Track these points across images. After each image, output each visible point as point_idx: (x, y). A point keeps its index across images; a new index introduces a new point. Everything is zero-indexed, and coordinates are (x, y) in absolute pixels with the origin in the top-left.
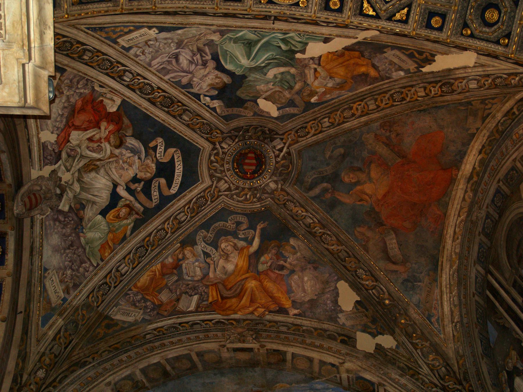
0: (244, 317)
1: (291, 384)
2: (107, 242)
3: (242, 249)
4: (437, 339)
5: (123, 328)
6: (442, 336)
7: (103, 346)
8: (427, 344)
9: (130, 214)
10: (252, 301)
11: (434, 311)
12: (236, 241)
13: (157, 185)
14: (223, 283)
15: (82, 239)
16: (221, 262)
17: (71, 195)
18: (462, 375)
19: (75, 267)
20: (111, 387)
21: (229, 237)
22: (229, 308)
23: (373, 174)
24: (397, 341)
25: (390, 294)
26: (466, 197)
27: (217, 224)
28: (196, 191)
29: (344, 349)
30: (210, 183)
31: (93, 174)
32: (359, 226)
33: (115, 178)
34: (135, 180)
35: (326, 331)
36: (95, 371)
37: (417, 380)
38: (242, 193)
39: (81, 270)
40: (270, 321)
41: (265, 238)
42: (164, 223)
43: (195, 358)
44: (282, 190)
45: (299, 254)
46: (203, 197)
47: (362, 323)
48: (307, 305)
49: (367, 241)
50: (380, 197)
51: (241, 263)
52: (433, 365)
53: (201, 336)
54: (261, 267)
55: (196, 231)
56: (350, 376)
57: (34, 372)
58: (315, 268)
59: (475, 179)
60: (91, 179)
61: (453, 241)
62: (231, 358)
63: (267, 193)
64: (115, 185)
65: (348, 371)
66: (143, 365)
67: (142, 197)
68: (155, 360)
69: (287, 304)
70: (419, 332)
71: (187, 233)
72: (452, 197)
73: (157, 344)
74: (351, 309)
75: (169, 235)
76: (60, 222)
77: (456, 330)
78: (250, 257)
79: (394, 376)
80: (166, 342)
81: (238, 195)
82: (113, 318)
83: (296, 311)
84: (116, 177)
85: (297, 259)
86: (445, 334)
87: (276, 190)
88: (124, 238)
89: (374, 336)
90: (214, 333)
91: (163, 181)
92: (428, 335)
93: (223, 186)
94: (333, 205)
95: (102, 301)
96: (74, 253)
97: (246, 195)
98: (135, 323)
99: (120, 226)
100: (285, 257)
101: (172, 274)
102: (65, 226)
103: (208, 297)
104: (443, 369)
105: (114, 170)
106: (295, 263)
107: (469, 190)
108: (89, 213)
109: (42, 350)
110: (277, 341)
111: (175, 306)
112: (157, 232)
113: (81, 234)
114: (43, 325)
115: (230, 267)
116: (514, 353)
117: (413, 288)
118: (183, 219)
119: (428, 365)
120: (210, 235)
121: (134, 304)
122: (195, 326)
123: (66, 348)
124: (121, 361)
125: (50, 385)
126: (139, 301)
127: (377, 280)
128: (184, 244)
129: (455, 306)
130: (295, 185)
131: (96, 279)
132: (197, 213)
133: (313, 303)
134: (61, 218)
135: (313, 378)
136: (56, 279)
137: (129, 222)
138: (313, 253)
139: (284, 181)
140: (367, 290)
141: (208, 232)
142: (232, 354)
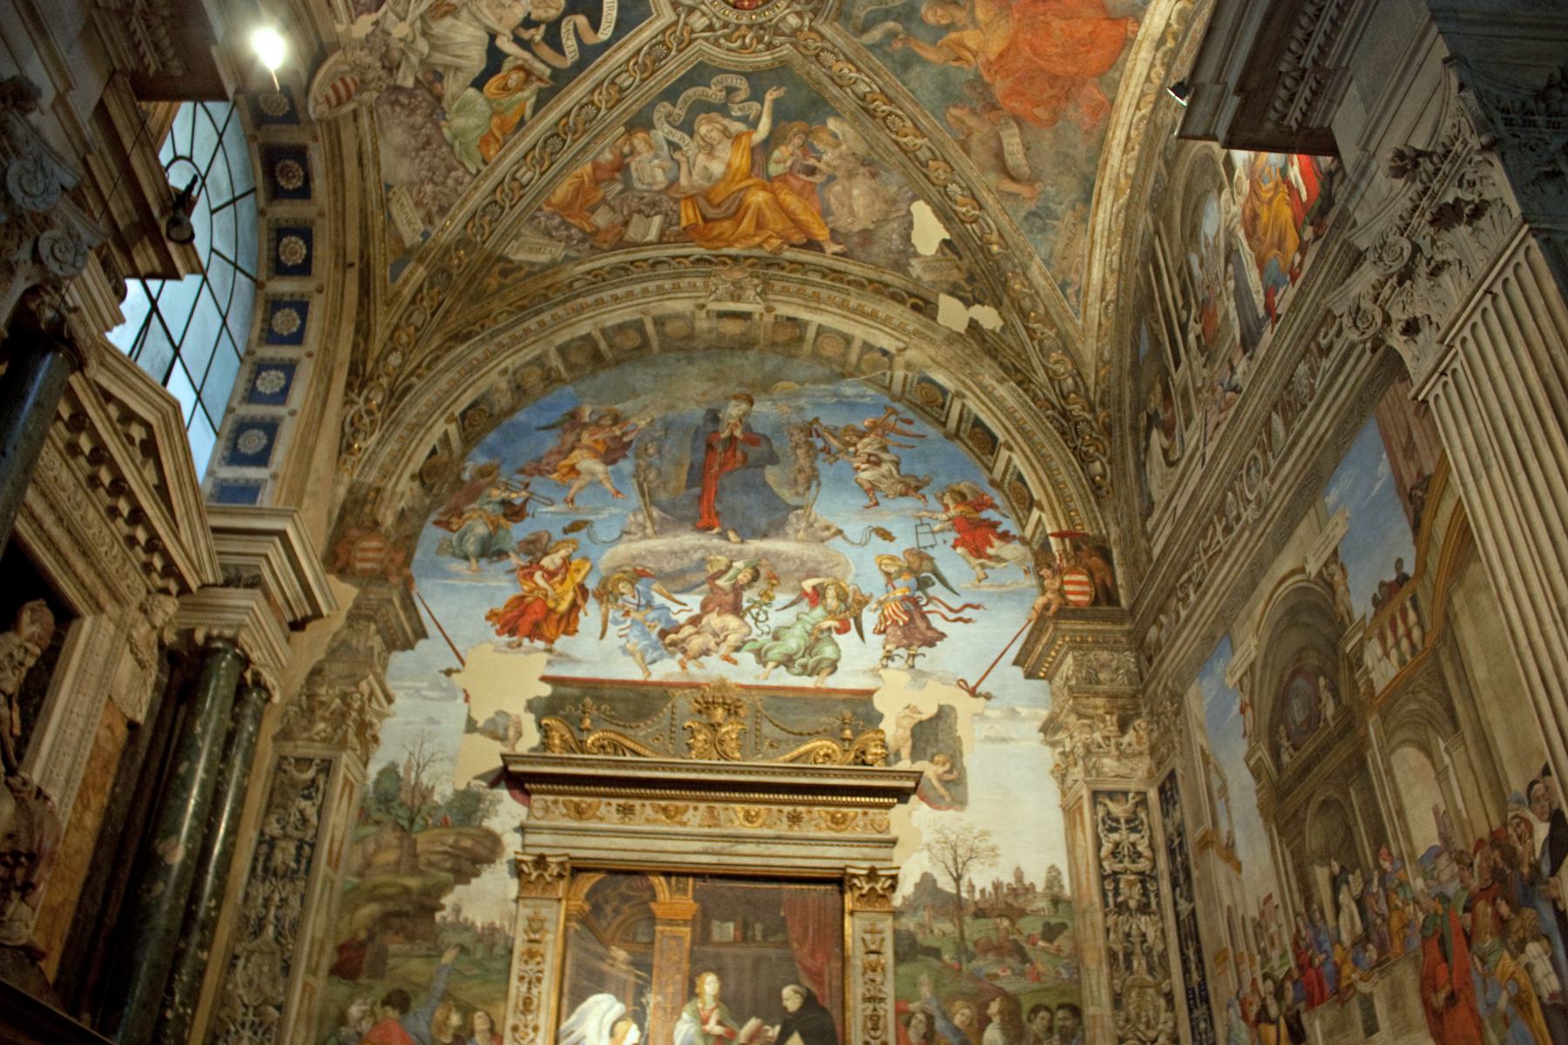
0: (746, 253)
1: (802, 383)
2: (491, 133)
3: (738, 137)
4: (1069, 327)
5: (529, 274)
6: (1079, 322)
7: (497, 305)
8: (1052, 333)
9: (527, 81)
10: (760, 225)
11: (1073, 276)
12: (726, 122)
13: (571, 27)
14: (706, 195)
15: (446, 131)
16: (702, 159)
17: (414, 59)
18: (1099, 395)
19: (438, 179)
20: (507, 377)
21: (713, 115)
22: (718, 237)
23: (980, 14)
24: (1004, 320)
25: (1001, 236)
26: (1153, 75)
27: (690, 92)
28: (646, 35)
29: (912, 320)
30: (674, 18)
31: (448, 21)
32: (955, 106)
33: (488, 22)
34: (528, 23)
35: (887, 285)
36: (484, 348)
37: (1026, 391)
38: (736, 35)
39: (450, 182)
40: (791, 262)
41: (781, 115)
42: (592, 92)
43: (650, 328)
44: (811, 29)
45: (844, 148)
46: (662, 43)
47: (951, 279)
48: (856, 239)
49: (968, 136)
50: (992, 57)
51: (737, 162)
52: (1054, 372)
53: (668, 284)
54: (774, 169)
55: (652, 105)
56: (910, 375)
57: (384, 356)
58: (874, 175)
59: (1170, 44)
60: (447, 30)
61: (1125, 152)
62: (710, 331)
63: (783, 34)
64: (493, 37)
65: (908, 366)
66: (563, 337)
67: (546, 51)
68: (583, 329)
69: (822, 235)
70: (1041, 310)
71: (635, 108)
72: (1127, 73)
73: (590, 300)
74: (932, 252)
75: (603, 112)
76: (402, 106)
77: (1106, 314)
78: (753, 150)
79: (988, 380)
80: (605, 295)
81: (728, 38)
82: (512, 257)
83: (837, 248)
84: (492, 22)
85: (841, 157)
86: (1085, 320)
87: (800, 29)
88: (522, 122)
89: (968, 304)
90: (692, 280)
91: (581, 20)
92: (1055, 317)
93: (698, 22)
94: (906, 63)
95: (491, 233)
96: (435, 156)
97: (744, 37)
98: (553, 264)
99: (511, 105)
100: (817, 151)
101: (613, 180)
102: (412, 112)
103: (679, 218)
104: (1070, 381)
105: (486, 11)
106: (835, 163)
107: (1158, 62)
108: (451, 86)
109: (395, 320)
110: (800, 301)
111: (621, 236)
112: (582, 108)
113: (443, 123)
114: (394, 277)
115: (717, 168)
116: (1158, 388)
117: (1043, 229)
118: (626, 84)
119: (1046, 369)
120: (680, 112)
121: (548, 233)
122: (659, 267)
123: (433, 314)
124: (527, 331)
125: (411, 374)
126: (557, 229)
127: (981, 208)
128: (631, 127)
129: (1112, 271)
130: (836, 20)
131: (477, 196)
132: (653, 72)
133: (867, 236)
134: (404, 100)
135: (843, 376)
136: (408, 201)
137: (528, 95)
138: (872, 148)
139: (816, 12)
140: (963, 222)
141: (674, 105)
142: (714, 323)
